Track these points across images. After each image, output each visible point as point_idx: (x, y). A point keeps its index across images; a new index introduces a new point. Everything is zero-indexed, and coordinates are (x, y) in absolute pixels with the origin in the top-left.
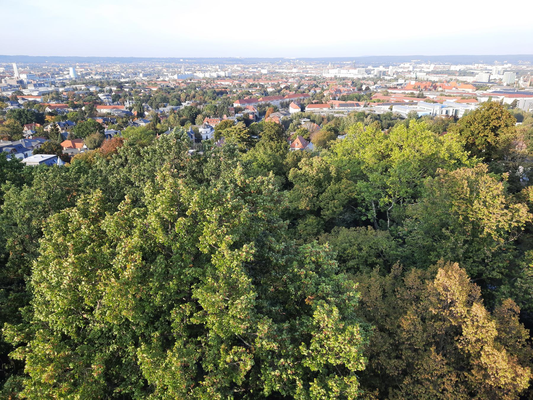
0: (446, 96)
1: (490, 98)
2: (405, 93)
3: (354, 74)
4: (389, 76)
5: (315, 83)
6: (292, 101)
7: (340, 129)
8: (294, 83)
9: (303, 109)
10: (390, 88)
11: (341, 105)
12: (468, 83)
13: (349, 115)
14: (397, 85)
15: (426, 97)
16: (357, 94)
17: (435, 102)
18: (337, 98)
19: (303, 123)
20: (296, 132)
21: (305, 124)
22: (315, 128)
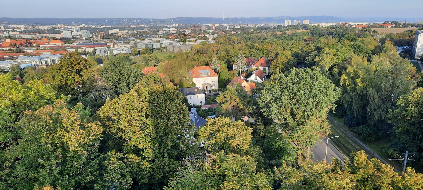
0: (41, 50)
1: (76, 49)
2: (3, 50)
12: (57, 39)
15: (24, 52)
17: (34, 55)
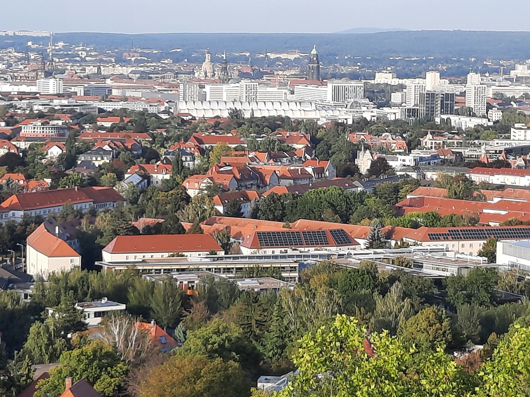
3: (313, 104)
4: (470, 113)
5: (145, 140)
6: (39, 221)
7: (267, 349)
8: (44, 142)
9: (91, 257)
10: (477, 165)
11: (264, 240)
13: (303, 281)
14: (509, 151)
16: (333, 190)
18: (247, 208)
19: (93, 321)
20: (60, 365)
21: (103, 324)
22: (148, 342)
